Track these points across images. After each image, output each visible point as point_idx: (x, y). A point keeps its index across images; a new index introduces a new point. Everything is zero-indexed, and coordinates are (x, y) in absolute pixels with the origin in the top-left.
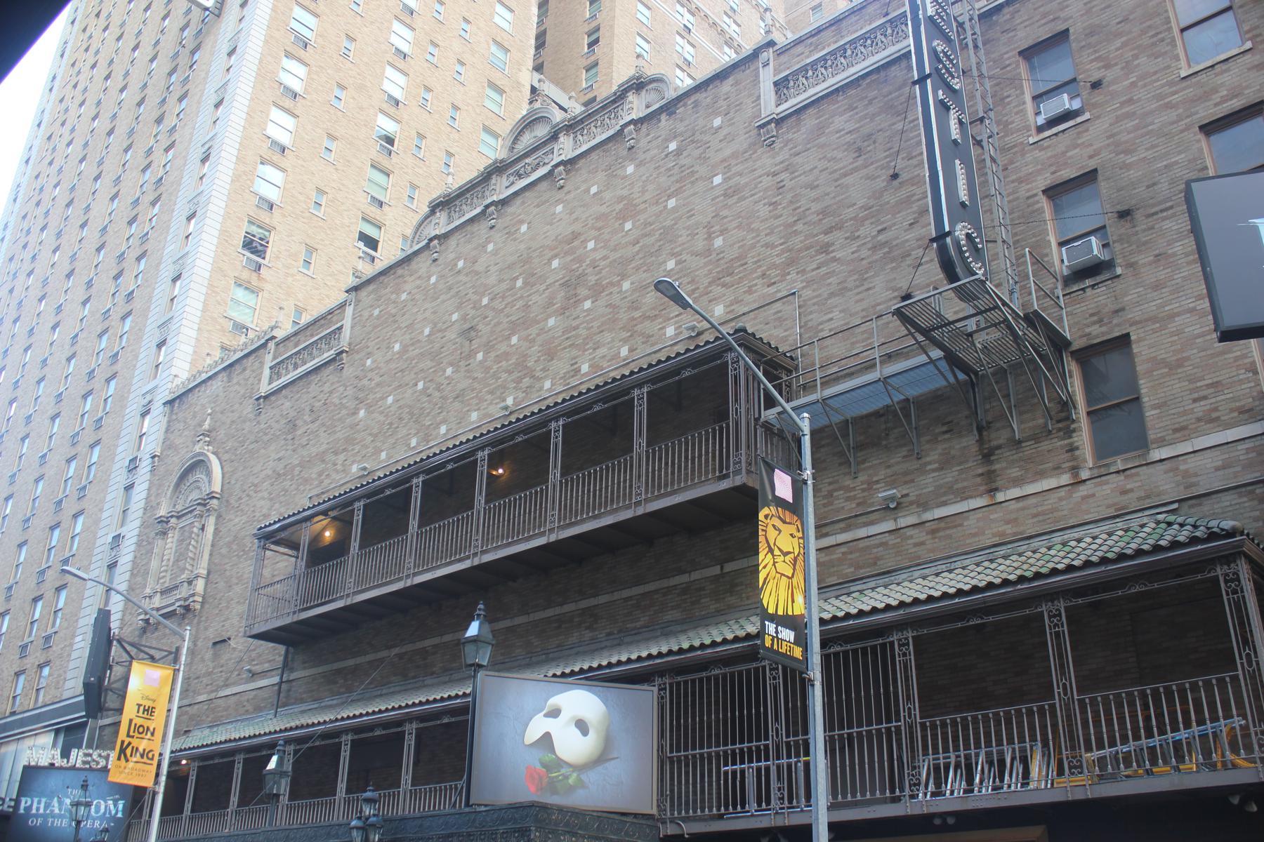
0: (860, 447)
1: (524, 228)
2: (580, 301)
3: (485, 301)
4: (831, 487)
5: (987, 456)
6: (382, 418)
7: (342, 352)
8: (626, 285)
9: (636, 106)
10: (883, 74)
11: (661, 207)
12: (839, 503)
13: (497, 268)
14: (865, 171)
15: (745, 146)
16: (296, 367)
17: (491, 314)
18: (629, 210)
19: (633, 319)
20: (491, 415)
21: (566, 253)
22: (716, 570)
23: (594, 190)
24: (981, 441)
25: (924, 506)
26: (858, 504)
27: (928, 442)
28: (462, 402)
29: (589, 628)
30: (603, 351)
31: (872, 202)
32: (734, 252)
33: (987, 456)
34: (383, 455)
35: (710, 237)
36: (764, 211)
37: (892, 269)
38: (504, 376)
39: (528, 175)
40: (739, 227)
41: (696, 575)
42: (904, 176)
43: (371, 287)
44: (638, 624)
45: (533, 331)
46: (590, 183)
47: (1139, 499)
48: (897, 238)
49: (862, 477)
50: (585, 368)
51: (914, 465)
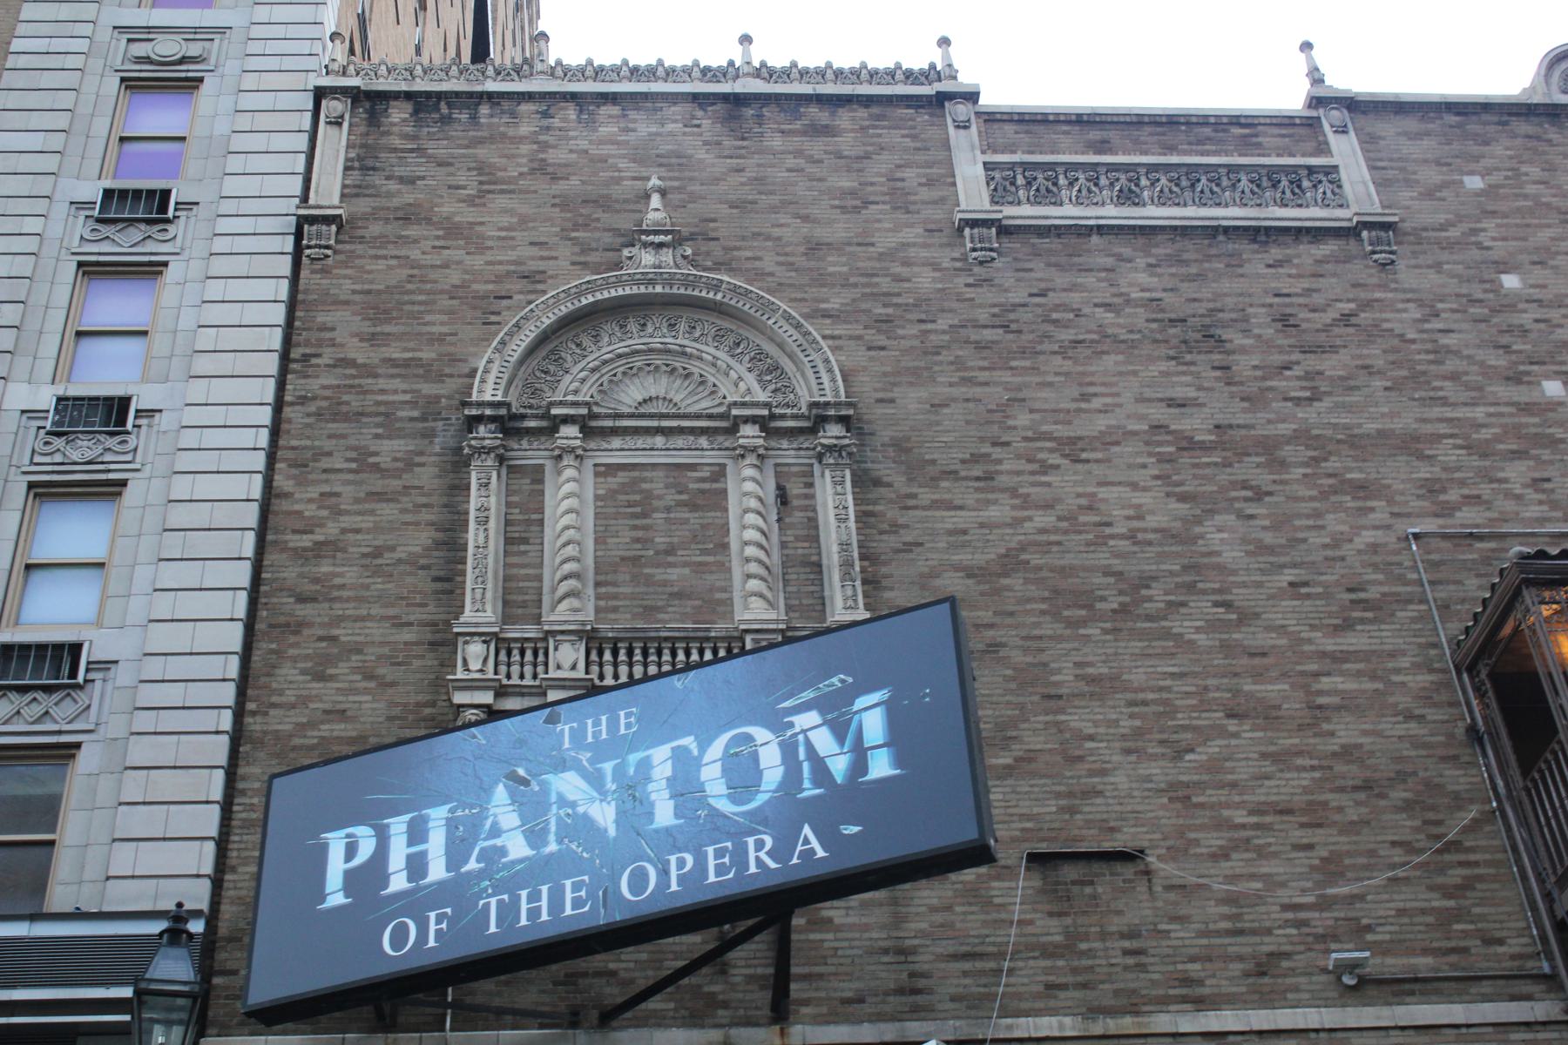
43: (1411, 124)
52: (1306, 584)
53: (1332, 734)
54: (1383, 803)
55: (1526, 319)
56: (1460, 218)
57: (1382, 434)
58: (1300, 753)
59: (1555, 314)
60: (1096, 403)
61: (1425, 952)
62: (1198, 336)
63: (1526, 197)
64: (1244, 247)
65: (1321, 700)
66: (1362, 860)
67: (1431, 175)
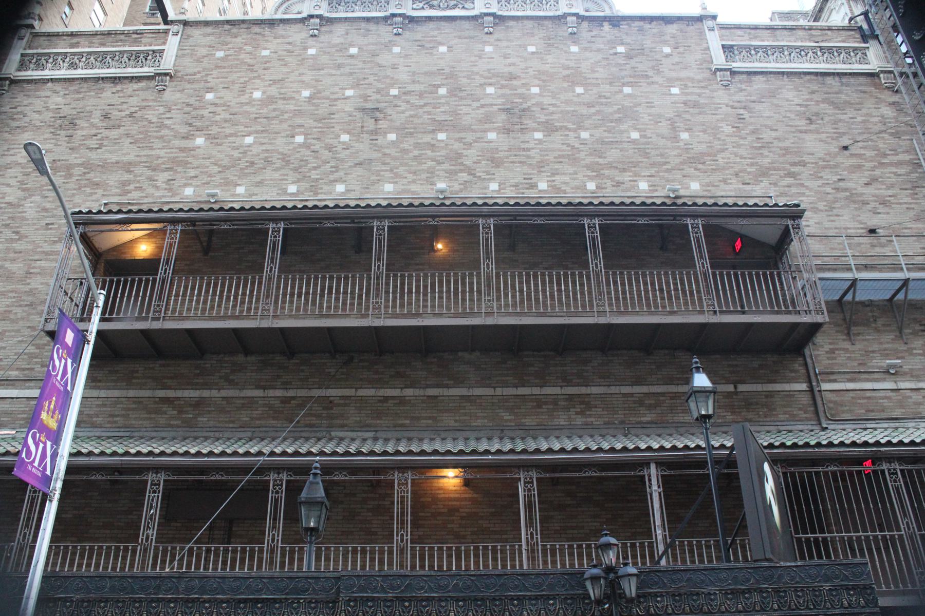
1: (443, 49)
3: (394, 92)
4: (831, 347)
6: (236, 154)
7: (166, 74)
8: (585, 135)
10: (820, 78)
11: (617, 89)
12: (839, 360)
13: (407, 69)
14: (819, 136)
15: (699, 77)
16: (73, 66)
17: (404, 106)
18: (574, 78)
20: (413, 193)
21: (503, 87)
22: (731, 388)
26: (860, 364)
27: (911, 334)
28: (370, 170)
29: (582, 413)
31: (828, 158)
34: (240, 190)
36: (728, 130)
37: (856, 208)
38: (430, 163)
39: (443, 9)
40: (704, 131)
42: (853, 150)
43: (209, 30)
44: (644, 419)
45: (470, 137)
48: (855, 189)
49: (858, 346)
50: (543, 186)
51: (904, 348)
52: (52, 224)
53: (29, 284)
54: (34, 311)
55: (205, 113)
56: (204, 69)
57: (117, 162)
58: (12, 292)
59: (218, 110)
60: (12, 152)
61: (17, 369)
62: (67, 123)
63: (238, 59)
64: (108, 85)
65: (32, 271)
66: (13, 333)
67: (203, 51)
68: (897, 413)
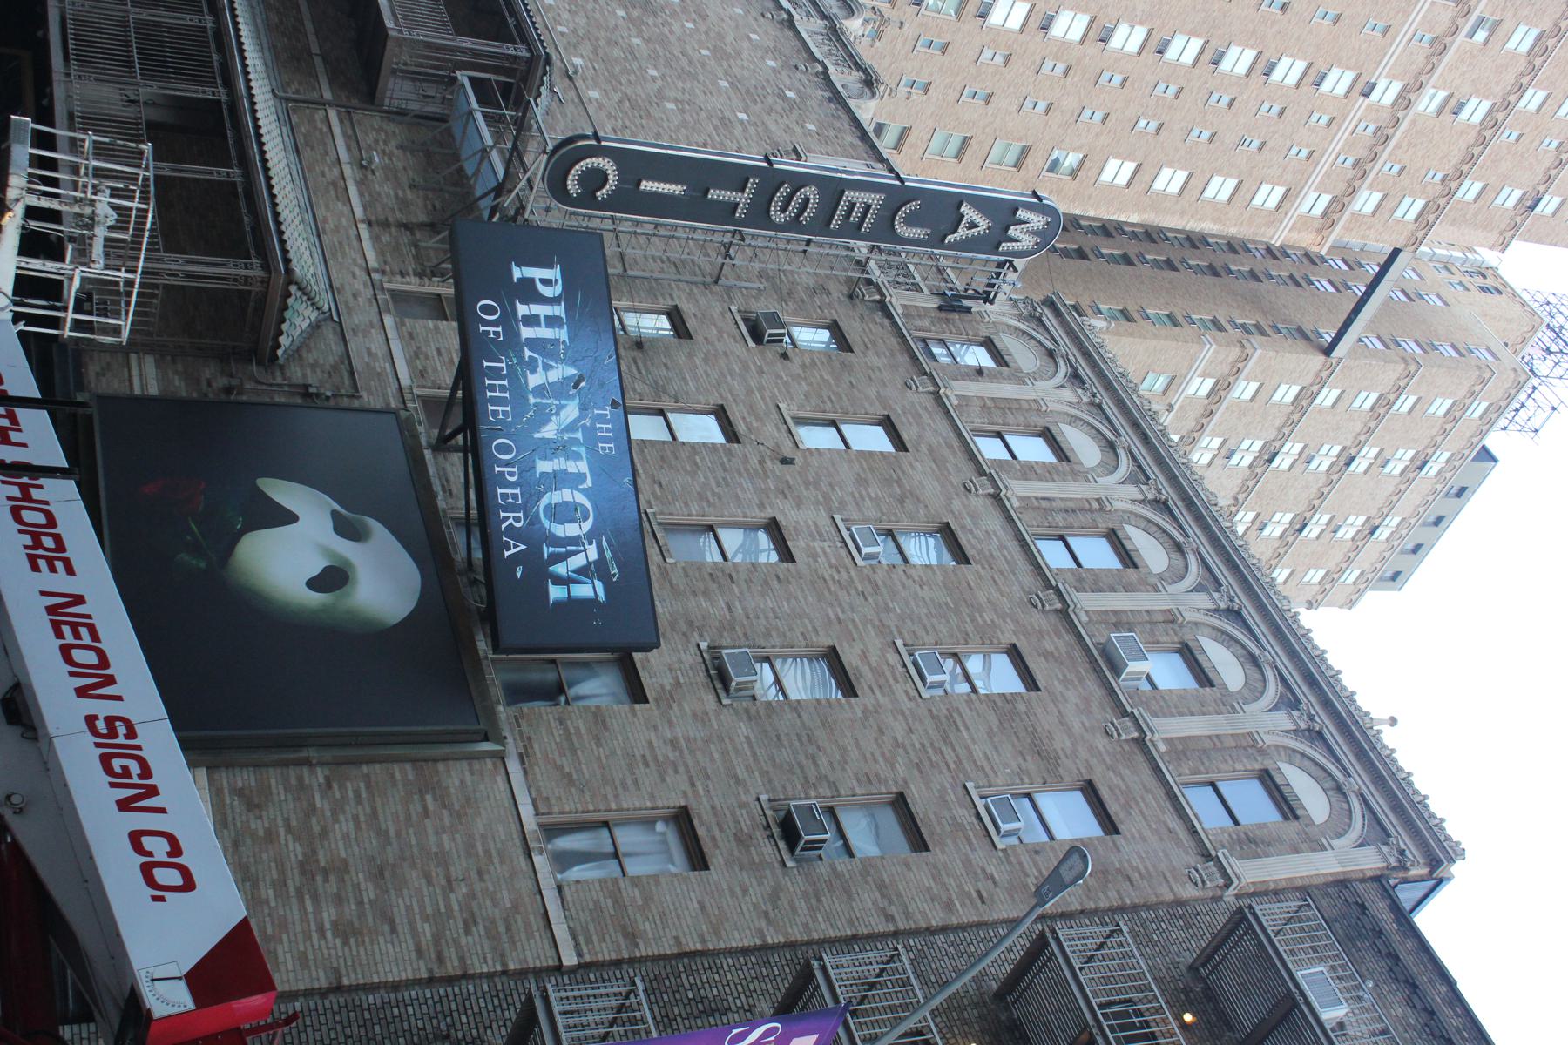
0: (428, 155)
2: (625, 8)
5: (406, 226)
9: (843, 78)
19: (597, 39)
22: (315, 49)
23: (754, 36)
24: (422, 225)
25: (360, 184)
30: (566, 15)
32: (655, 112)
33: (406, 226)
35: (676, 101)
41: (312, 38)
46: (763, 33)
47: (347, 304)
68: (307, 153)
